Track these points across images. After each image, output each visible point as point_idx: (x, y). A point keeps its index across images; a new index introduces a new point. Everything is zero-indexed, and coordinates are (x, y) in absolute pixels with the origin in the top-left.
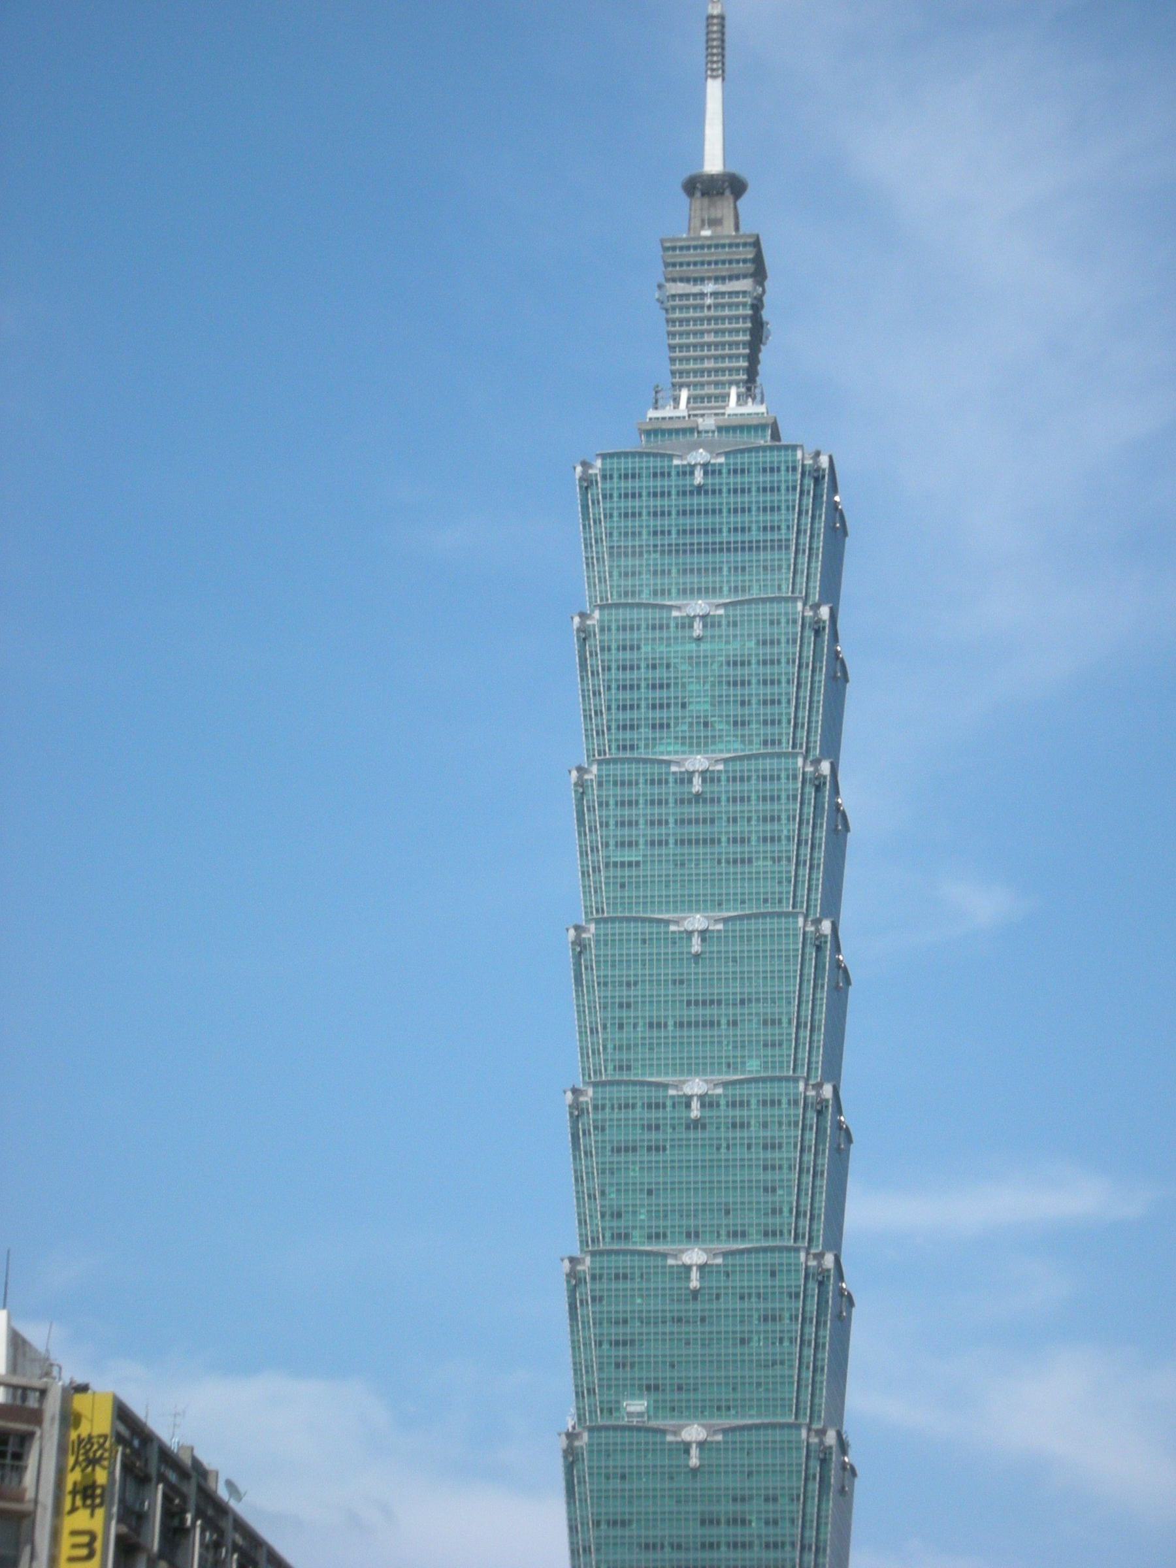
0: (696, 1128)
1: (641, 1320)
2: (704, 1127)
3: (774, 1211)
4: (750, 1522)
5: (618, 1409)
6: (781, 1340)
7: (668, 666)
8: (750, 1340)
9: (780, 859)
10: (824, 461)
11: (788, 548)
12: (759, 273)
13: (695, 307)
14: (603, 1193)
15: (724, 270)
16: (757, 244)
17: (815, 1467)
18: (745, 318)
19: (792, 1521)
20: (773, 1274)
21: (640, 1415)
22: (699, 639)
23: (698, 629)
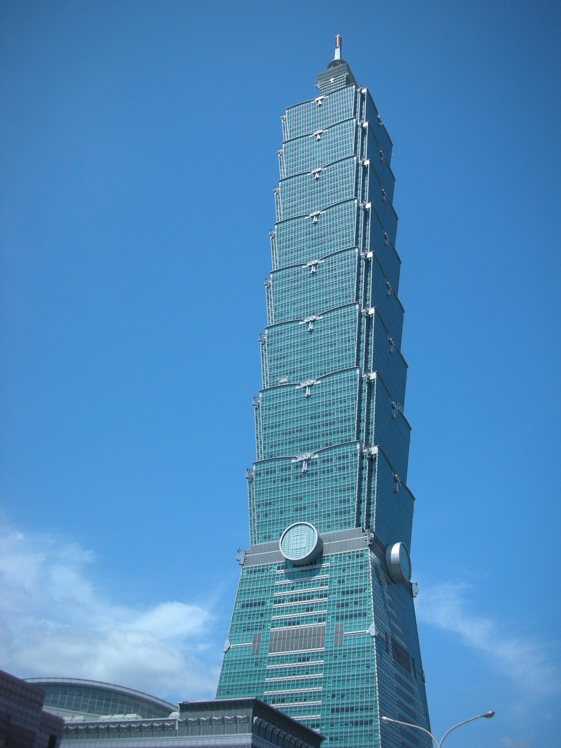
0: (313, 276)
1: (288, 348)
2: (317, 275)
3: (346, 297)
4: (334, 414)
5: (277, 384)
6: (349, 341)
7: (308, 150)
8: (335, 344)
9: (349, 188)
10: (364, 91)
11: (351, 110)
12: (349, 70)
13: (328, 85)
14: (275, 309)
15: (336, 75)
16: (348, 65)
17: (365, 387)
18: (343, 82)
19: (353, 408)
20: (345, 316)
21: (286, 383)
22: (319, 140)
23: (319, 137)
